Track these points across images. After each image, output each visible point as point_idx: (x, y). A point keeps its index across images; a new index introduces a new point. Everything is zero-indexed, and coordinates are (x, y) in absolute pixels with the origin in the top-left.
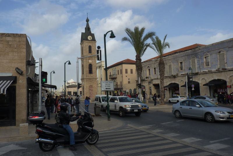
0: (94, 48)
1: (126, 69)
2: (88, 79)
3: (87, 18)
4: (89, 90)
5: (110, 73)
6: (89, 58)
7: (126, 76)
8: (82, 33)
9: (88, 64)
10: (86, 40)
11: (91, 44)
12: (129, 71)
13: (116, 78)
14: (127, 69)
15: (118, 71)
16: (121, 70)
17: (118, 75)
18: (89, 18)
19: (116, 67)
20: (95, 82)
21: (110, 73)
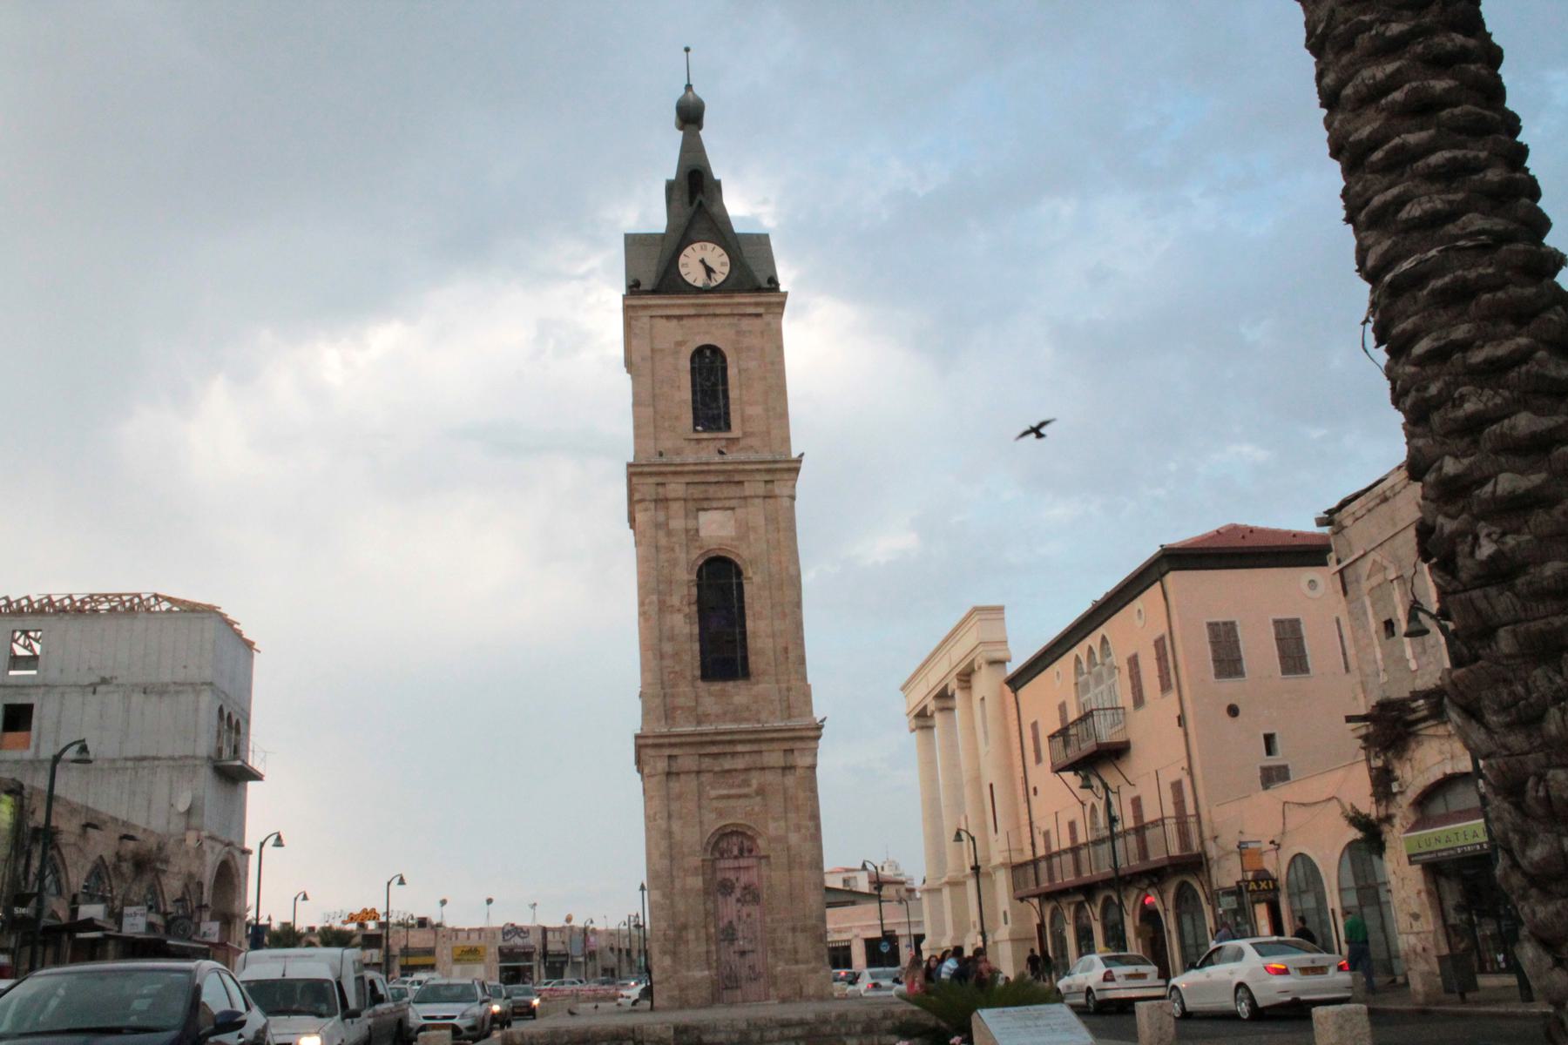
0: (753, 364)
1: (1210, 625)
2: (699, 743)
3: (689, 87)
4: (706, 892)
5: (1062, 708)
6: (697, 492)
7: (1233, 711)
8: (635, 244)
9: (696, 556)
10: (655, 291)
11: (716, 333)
12: (1259, 649)
13: (1115, 753)
14: (1230, 627)
15: (1133, 662)
16: (1159, 644)
17: (1142, 711)
18: (699, 91)
19: (1101, 631)
20: (790, 780)
21: (1062, 708)
